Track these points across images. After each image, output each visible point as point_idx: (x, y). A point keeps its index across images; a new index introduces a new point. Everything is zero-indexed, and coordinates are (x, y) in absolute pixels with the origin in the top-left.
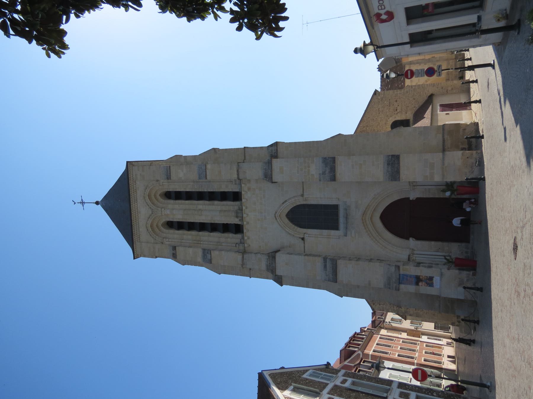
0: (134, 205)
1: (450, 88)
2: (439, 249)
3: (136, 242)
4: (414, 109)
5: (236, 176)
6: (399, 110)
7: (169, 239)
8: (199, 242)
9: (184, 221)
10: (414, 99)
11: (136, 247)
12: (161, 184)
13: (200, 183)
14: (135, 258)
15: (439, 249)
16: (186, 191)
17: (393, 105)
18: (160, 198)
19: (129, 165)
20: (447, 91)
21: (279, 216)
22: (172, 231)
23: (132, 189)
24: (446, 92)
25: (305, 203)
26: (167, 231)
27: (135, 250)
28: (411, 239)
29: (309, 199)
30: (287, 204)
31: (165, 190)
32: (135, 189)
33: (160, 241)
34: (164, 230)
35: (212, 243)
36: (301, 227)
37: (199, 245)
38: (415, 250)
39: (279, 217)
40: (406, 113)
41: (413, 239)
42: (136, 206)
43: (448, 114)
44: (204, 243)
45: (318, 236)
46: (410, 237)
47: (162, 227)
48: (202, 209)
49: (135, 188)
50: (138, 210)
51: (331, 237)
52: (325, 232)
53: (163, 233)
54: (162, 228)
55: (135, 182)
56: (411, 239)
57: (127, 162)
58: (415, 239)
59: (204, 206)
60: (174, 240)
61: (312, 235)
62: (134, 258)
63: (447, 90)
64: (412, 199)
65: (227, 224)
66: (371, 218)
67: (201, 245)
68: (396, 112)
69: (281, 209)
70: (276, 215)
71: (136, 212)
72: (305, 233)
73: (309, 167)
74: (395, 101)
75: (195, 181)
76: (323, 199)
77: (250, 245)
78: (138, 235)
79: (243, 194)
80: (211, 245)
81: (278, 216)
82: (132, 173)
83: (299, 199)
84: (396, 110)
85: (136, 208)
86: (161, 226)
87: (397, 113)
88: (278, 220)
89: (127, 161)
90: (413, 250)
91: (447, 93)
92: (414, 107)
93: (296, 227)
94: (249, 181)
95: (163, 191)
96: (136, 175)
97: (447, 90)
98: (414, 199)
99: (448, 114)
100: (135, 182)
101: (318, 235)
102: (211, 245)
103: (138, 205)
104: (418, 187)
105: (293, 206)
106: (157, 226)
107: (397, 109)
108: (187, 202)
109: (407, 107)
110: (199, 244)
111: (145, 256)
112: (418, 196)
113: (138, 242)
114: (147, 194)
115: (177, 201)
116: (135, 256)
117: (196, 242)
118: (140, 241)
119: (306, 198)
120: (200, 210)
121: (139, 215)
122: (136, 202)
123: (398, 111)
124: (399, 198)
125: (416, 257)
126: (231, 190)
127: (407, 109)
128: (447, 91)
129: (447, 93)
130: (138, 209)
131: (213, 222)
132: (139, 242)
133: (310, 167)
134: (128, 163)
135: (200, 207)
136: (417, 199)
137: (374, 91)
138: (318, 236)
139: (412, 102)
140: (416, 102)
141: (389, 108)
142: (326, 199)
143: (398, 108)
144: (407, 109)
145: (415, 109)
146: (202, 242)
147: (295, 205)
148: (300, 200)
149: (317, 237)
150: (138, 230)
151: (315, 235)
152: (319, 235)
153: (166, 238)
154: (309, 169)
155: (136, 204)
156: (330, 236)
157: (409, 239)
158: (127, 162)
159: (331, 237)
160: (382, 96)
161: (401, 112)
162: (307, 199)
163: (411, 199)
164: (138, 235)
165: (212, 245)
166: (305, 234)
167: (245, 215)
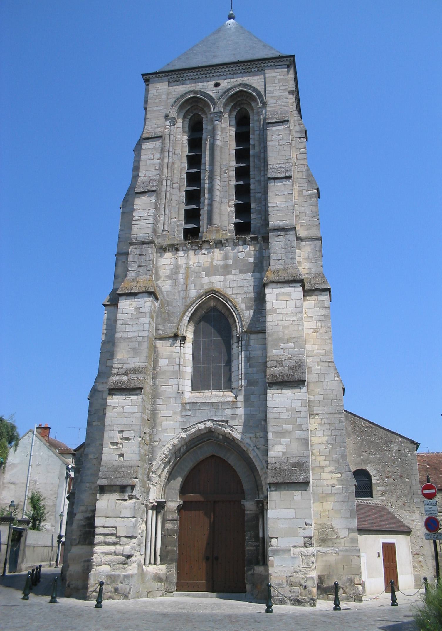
3: (169, 77)
14: (144, 77)
43: (379, 556)
57: (293, 56)
62: (143, 75)
82: (276, 65)
89: (294, 55)
99: (379, 556)
116: (147, 77)
122: (230, 74)
134: (292, 58)
158: (293, 56)
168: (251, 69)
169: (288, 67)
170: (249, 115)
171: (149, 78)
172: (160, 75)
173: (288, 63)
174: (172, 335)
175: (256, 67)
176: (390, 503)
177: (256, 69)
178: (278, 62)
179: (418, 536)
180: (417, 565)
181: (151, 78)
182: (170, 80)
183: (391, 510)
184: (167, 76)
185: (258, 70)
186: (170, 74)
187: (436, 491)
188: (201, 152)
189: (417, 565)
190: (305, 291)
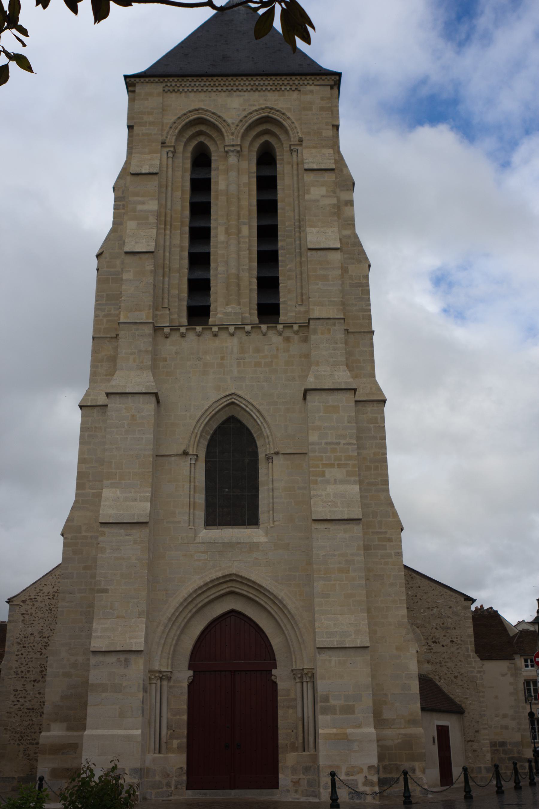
0: (247, 83)
1: (475, 746)
2: (174, 731)
3: (164, 85)
4: (437, 677)
5: (316, 315)
6: (434, 648)
7: (173, 158)
8: (168, 227)
9: (213, 193)
10: (456, 677)
11: (152, 83)
12: (292, 147)
13: (297, 234)
14: (128, 80)
15: (174, 731)
16: (278, 201)
17: (445, 636)
18: (261, 142)
19: (333, 77)
20: (470, 741)
21: (233, 403)
22: (188, 165)
23: (281, 82)
24: (468, 739)
25: (261, 456)
26: (189, 155)
27: (145, 79)
28: (191, 673)
29: (270, 464)
30: (259, 419)
31: (278, 154)
32: (281, 89)
33: (167, 137)
34: (190, 148)
35: (167, 254)
36: (208, 446)
37: (163, 226)
38: (168, 683)
39: (230, 401)
40: (428, 662)
41: (192, 678)
42: (245, 88)
43: (434, 742)
44: (168, 237)
45: (192, 484)
46: (194, 672)
47: (196, 142)
48: (240, 235)
49: (283, 88)
50: (235, 91)
51: (192, 510)
52: (200, 499)
53: (185, 145)
54: (194, 143)
55: (296, 89)
56: (191, 673)
57: (339, 75)
58: (190, 681)
59: (247, 240)
60: (170, 170)
61: (195, 472)
62: (126, 77)
63: (473, 741)
64: (273, 674)
65: (209, 289)
66: (232, 593)
67: (163, 231)
68: (430, 643)
69: (247, 406)
70: (234, 397)
71: (230, 88)
72: (197, 456)
73: (340, 466)
74: (453, 640)
75: (302, 223)
76: (271, 494)
77: (167, 337)
78: (180, 89)
79: (276, 327)
80: (164, 252)
81: (233, 400)
82: (315, 84)
83: (269, 444)
84: (434, 642)
85: (240, 88)
86: (199, 141)
87: (428, 644)
88: (224, 400)
90: (169, 679)
91: (468, 741)
92: (440, 678)
93: (209, 437)
94: (306, 340)
95: (277, 150)
96: (311, 92)
97: (473, 741)
98: (273, 677)
99: (434, 742)
100: (296, 89)
101: (195, 483)
102: (164, 252)
103: (246, 94)
104: (299, 685)
105: (252, 431)
106: (200, 133)
107: (436, 643)
108: (255, 202)
109: (440, 663)
110: (165, 226)
111: (131, 101)
112: (281, 686)
113: (164, 87)
114: (270, 115)
115: (255, 180)
116: (132, 80)
117: (168, 219)
118: (166, 92)
119: (272, 458)
120: (239, 231)
121: (223, 94)
123: (433, 645)
124: (275, 648)
125: (156, 684)
126: (281, 300)
127: (436, 663)
128: (470, 741)
129: (468, 741)
130: (238, 93)
131: (212, 257)
132: (164, 90)
133: (340, 468)
134: (337, 78)
135: (245, 230)
136: (275, 684)
137: (472, 597)
138: (192, 484)
139: (451, 672)
140: (449, 681)
141: (438, 627)
142: (271, 501)
143: (438, 644)
144: (436, 663)
145: (435, 679)
146: (168, 232)
147: (255, 435)
148: (268, 446)
149: (190, 482)
150: (190, 90)
151: (195, 478)
152: (194, 486)
153: (174, 152)
154: (336, 467)
155: (247, 88)
156: (194, 510)
157: (191, 670)
158: (339, 75)
159: (192, 510)
160: (462, 614)
161: (431, 652)
162: (270, 460)
163: (274, 672)
164: (180, 89)
165: (164, 256)
166: (196, 457)
167: (234, 330)
168: (281, 85)
169: (332, 87)
170: (275, 153)
171: (135, 82)
172: (152, 79)
173: (332, 83)
174: (180, 452)
175: (288, 84)
176: (438, 675)
177: (288, 88)
178: (318, 80)
179: (473, 718)
180: (470, 755)
181: (138, 83)
182: (166, 89)
183: (439, 684)
184: (162, 82)
185: (291, 89)
186: (166, 79)
187: (535, 660)
188: (210, 199)
189: (470, 755)
190: (356, 402)
